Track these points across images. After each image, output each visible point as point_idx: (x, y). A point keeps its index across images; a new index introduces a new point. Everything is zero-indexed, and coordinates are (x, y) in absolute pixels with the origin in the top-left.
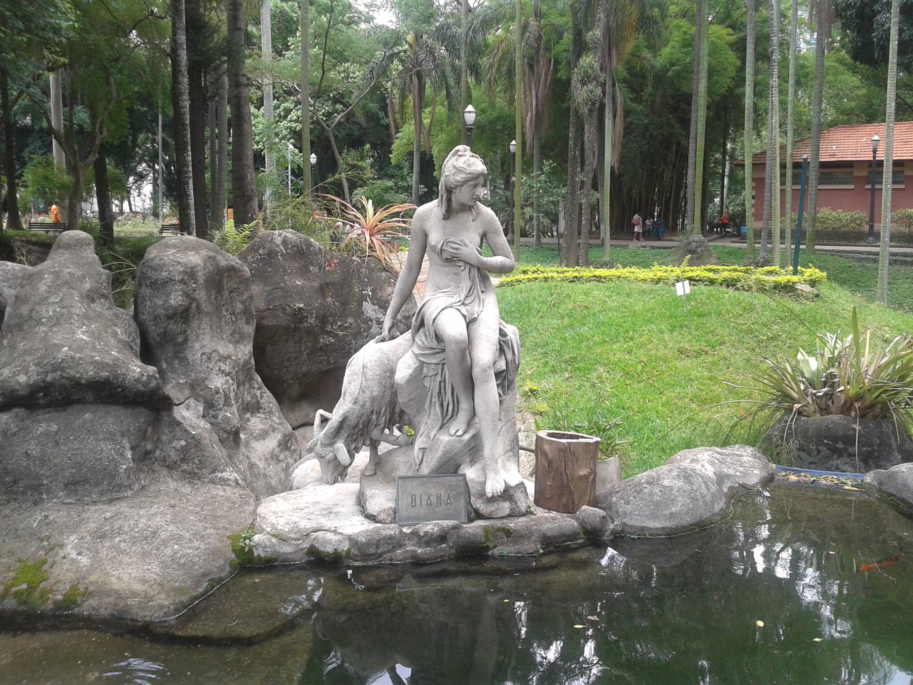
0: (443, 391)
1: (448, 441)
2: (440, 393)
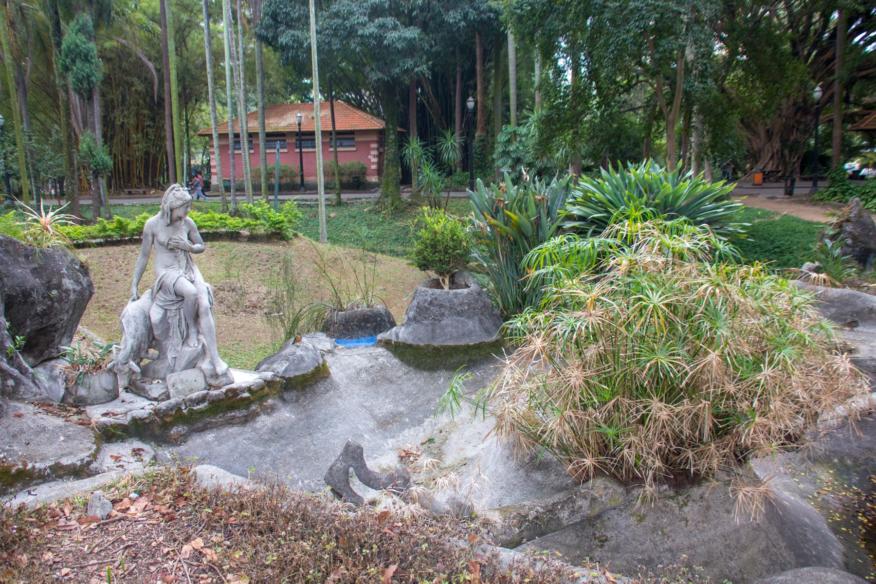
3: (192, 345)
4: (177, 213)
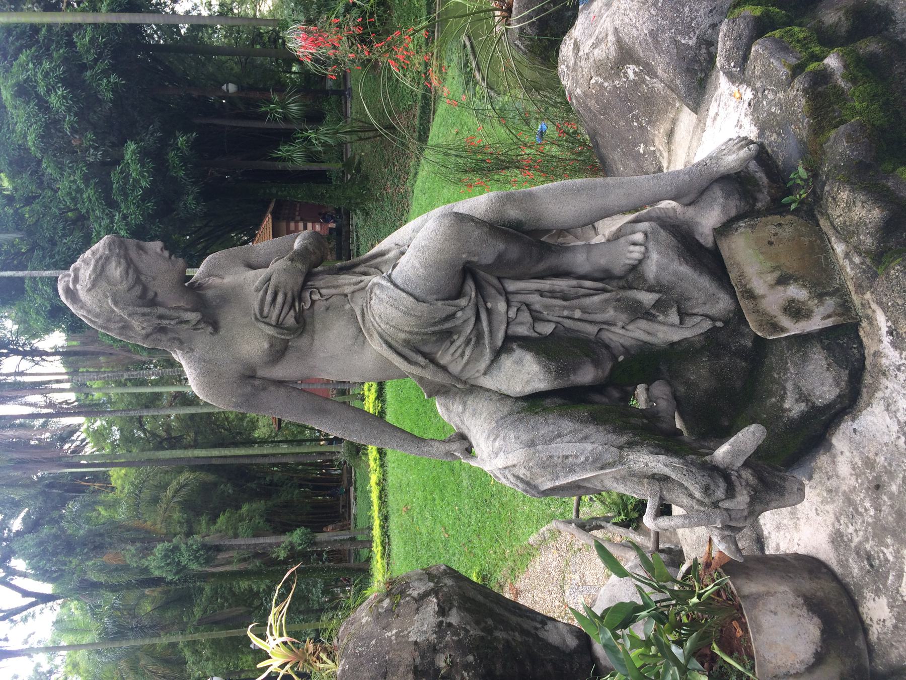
1: (660, 253)
2: (565, 298)
3: (636, 253)
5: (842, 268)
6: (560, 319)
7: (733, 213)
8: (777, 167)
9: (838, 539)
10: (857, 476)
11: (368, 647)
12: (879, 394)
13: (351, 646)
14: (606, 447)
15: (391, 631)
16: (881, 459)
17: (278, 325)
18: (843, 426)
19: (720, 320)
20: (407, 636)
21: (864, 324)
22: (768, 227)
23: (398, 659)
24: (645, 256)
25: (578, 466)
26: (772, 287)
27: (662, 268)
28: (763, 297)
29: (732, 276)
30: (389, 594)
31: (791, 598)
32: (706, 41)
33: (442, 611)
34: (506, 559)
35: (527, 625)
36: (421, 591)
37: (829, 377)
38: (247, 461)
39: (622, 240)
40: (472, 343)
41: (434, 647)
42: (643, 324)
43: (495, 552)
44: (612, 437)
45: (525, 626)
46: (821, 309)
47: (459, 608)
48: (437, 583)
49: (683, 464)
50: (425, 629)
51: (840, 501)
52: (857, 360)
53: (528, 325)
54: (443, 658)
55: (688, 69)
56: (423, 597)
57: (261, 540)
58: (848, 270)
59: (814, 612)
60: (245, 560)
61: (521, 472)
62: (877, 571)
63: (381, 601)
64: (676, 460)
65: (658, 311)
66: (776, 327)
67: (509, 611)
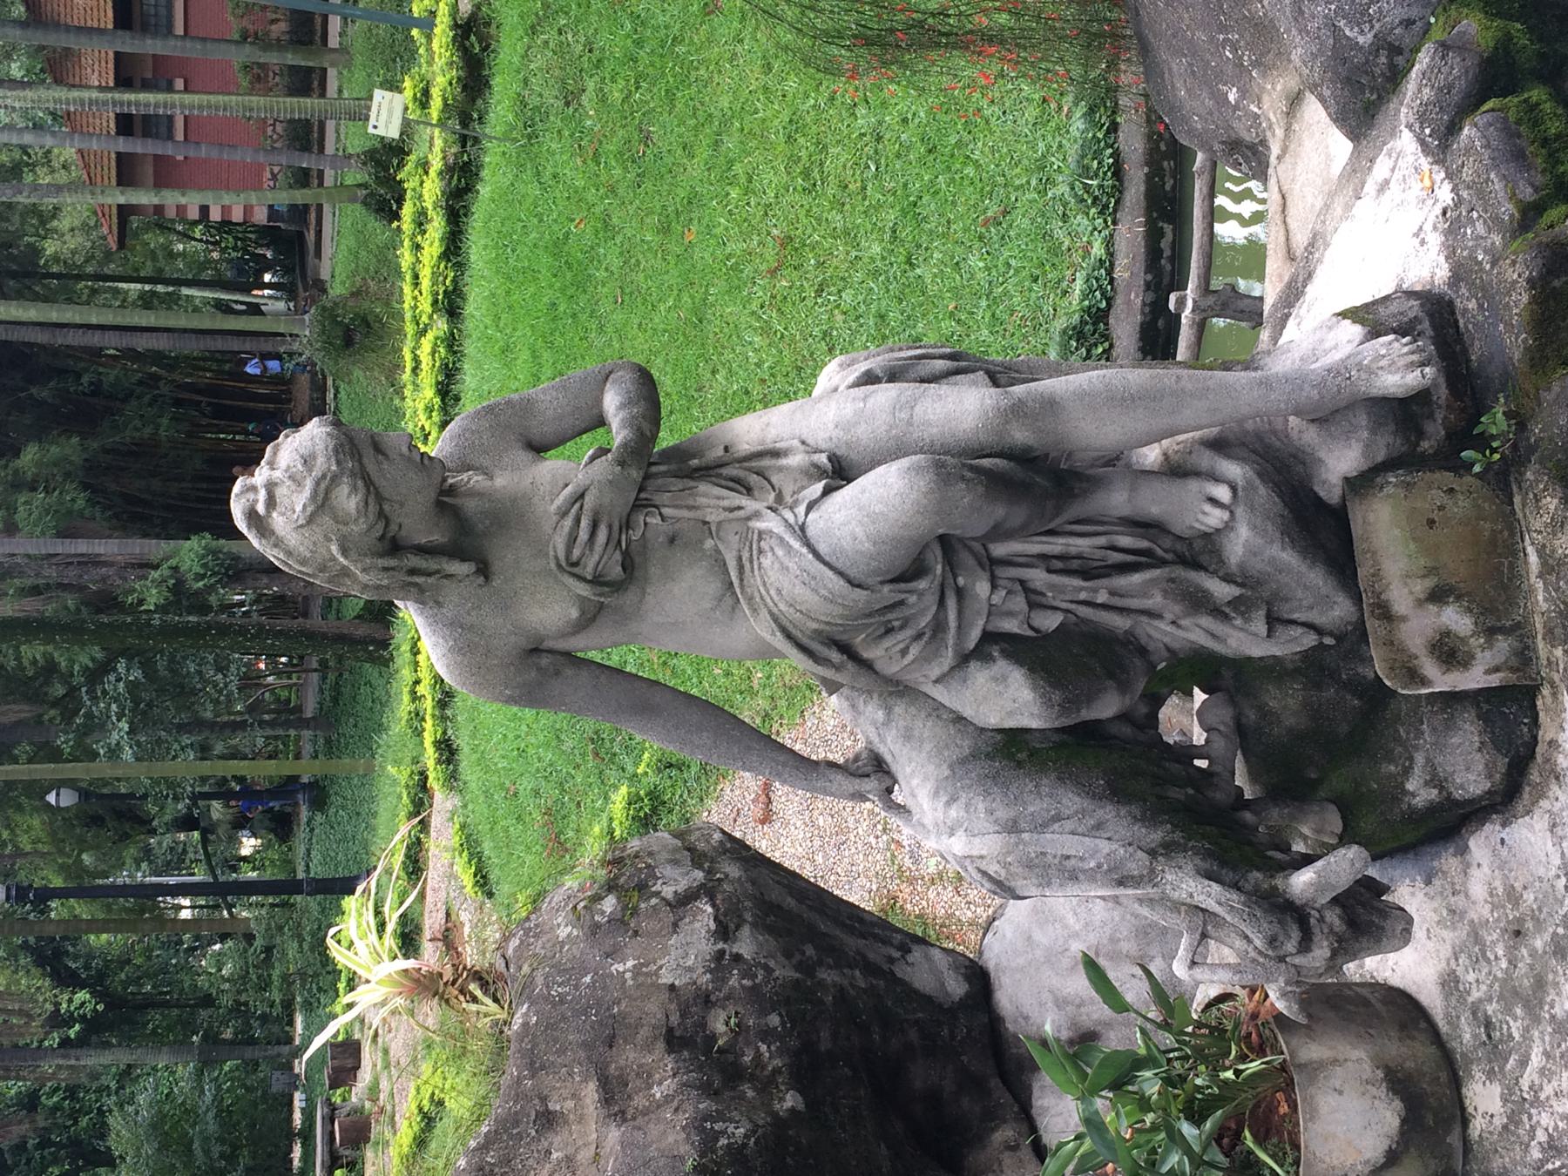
0: (1075, 564)
1: (1253, 527)
2: (1087, 573)
4: (419, 526)
5: (1531, 591)
6: (1073, 607)
7: (1381, 456)
8: (1468, 361)
9: (1450, 983)
10: (1494, 907)
11: (576, 987)
12: (1545, 804)
13: (540, 980)
14: (1131, 849)
15: (623, 961)
16: (1529, 897)
17: (597, 581)
18: (1488, 827)
19: (1331, 634)
20: (656, 973)
21: (1546, 691)
22: (1433, 490)
23: (637, 1014)
24: (1229, 526)
25: (1084, 871)
26: (1420, 603)
27: (1252, 552)
28: (1404, 619)
29: (1361, 572)
30: (611, 886)
31: (1367, 1070)
32: (1390, 44)
33: (723, 931)
34: (753, 693)
35: (877, 953)
36: (681, 888)
37: (1479, 762)
38: (41, 337)
39: (1193, 485)
40: (925, 638)
41: (708, 996)
42: (1206, 621)
43: (728, 674)
44: (1139, 831)
45: (871, 956)
46: (1488, 654)
47: (754, 925)
48: (709, 872)
49: (1244, 904)
50: (690, 963)
51: (1463, 932)
52: (1525, 744)
53: (1021, 617)
54: (723, 1016)
55: (1348, 79)
56: (685, 900)
57: (82, 547)
58: (1540, 598)
59: (1396, 1092)
60: (35, 591)
61: (993, 869)
62: (1495, 1048)
63: (597, 898)
64: (1235, 897)
65: (1236, 610)
66: (1414, 676)
67: (843, 925)
